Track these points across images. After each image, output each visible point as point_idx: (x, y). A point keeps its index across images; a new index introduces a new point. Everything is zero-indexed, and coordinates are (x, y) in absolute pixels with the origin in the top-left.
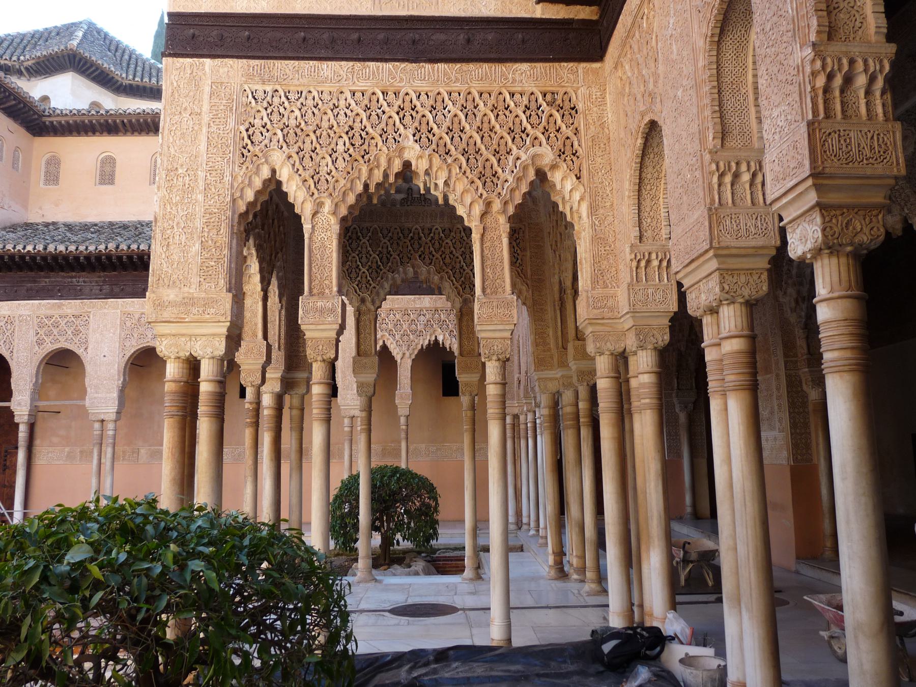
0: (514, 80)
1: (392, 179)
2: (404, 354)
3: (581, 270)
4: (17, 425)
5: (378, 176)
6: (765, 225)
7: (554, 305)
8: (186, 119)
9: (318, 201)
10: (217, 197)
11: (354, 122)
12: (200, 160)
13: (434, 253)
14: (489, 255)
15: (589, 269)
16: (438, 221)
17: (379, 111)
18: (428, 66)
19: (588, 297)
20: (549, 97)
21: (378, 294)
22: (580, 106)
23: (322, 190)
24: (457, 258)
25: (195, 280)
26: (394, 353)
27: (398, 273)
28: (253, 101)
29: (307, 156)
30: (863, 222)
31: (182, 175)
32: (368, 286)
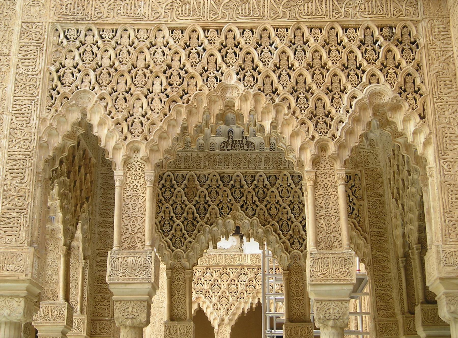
1: (213, 120)
2: (223, 320)
3: (430, 221)
5: (198, 119)
7: (398, 263)
9: (131, 145)
11: (172, 60)
12: (6, 103)
13: (258, 203)
15: (439, 220)
16: (262, 166)
17: (200, 49)
19: (438, 252)
20: (386, 31)
21: (193, 249)
22: (422, 41)
23: (137, 133)
24: (285, 208)
26: (211, 318)
27: (217, 225)
28: (65, 41)
29: (121, 96)
32: (183, 240)
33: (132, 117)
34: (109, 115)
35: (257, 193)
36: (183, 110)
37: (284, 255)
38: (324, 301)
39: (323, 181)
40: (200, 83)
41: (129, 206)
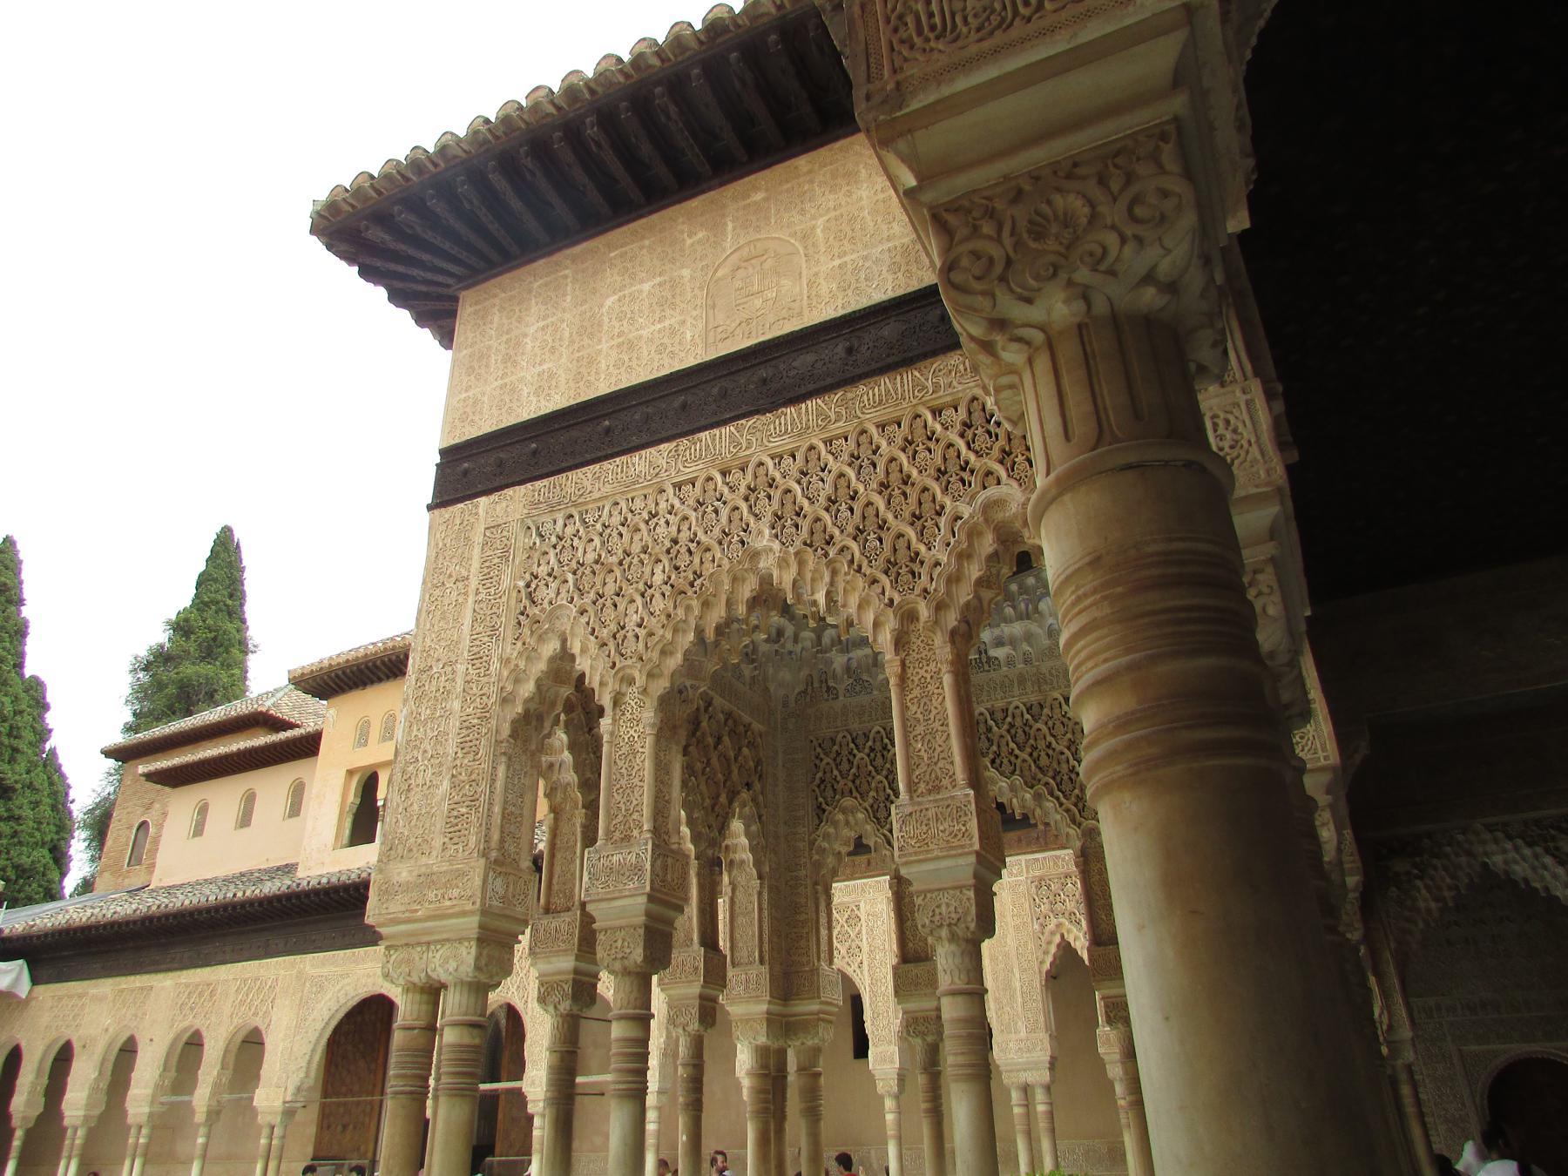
0: (937, 387)
1: (741, 610)
4: (530, 1118)
5: (718, 614)
6: (1228, 435)
8: (448, 591)
9: (620, 675)
10: (478, 700)
13: (1017, 752)
14: (919, 715)
16: (1016, 692)
18: (791, 411)
23: (629, 654)
24: (1062, 753)
25: (438, 842)
30: (1096, 193)
31: (436, 676)
33: (624, 632)
34: (592, 634)
35: (1013, 738)
36: (695, 604)
37: (1071, 832)
38: (930, 891)
39: (915, 673)
40: (718, 555)
41: (623, 771)
